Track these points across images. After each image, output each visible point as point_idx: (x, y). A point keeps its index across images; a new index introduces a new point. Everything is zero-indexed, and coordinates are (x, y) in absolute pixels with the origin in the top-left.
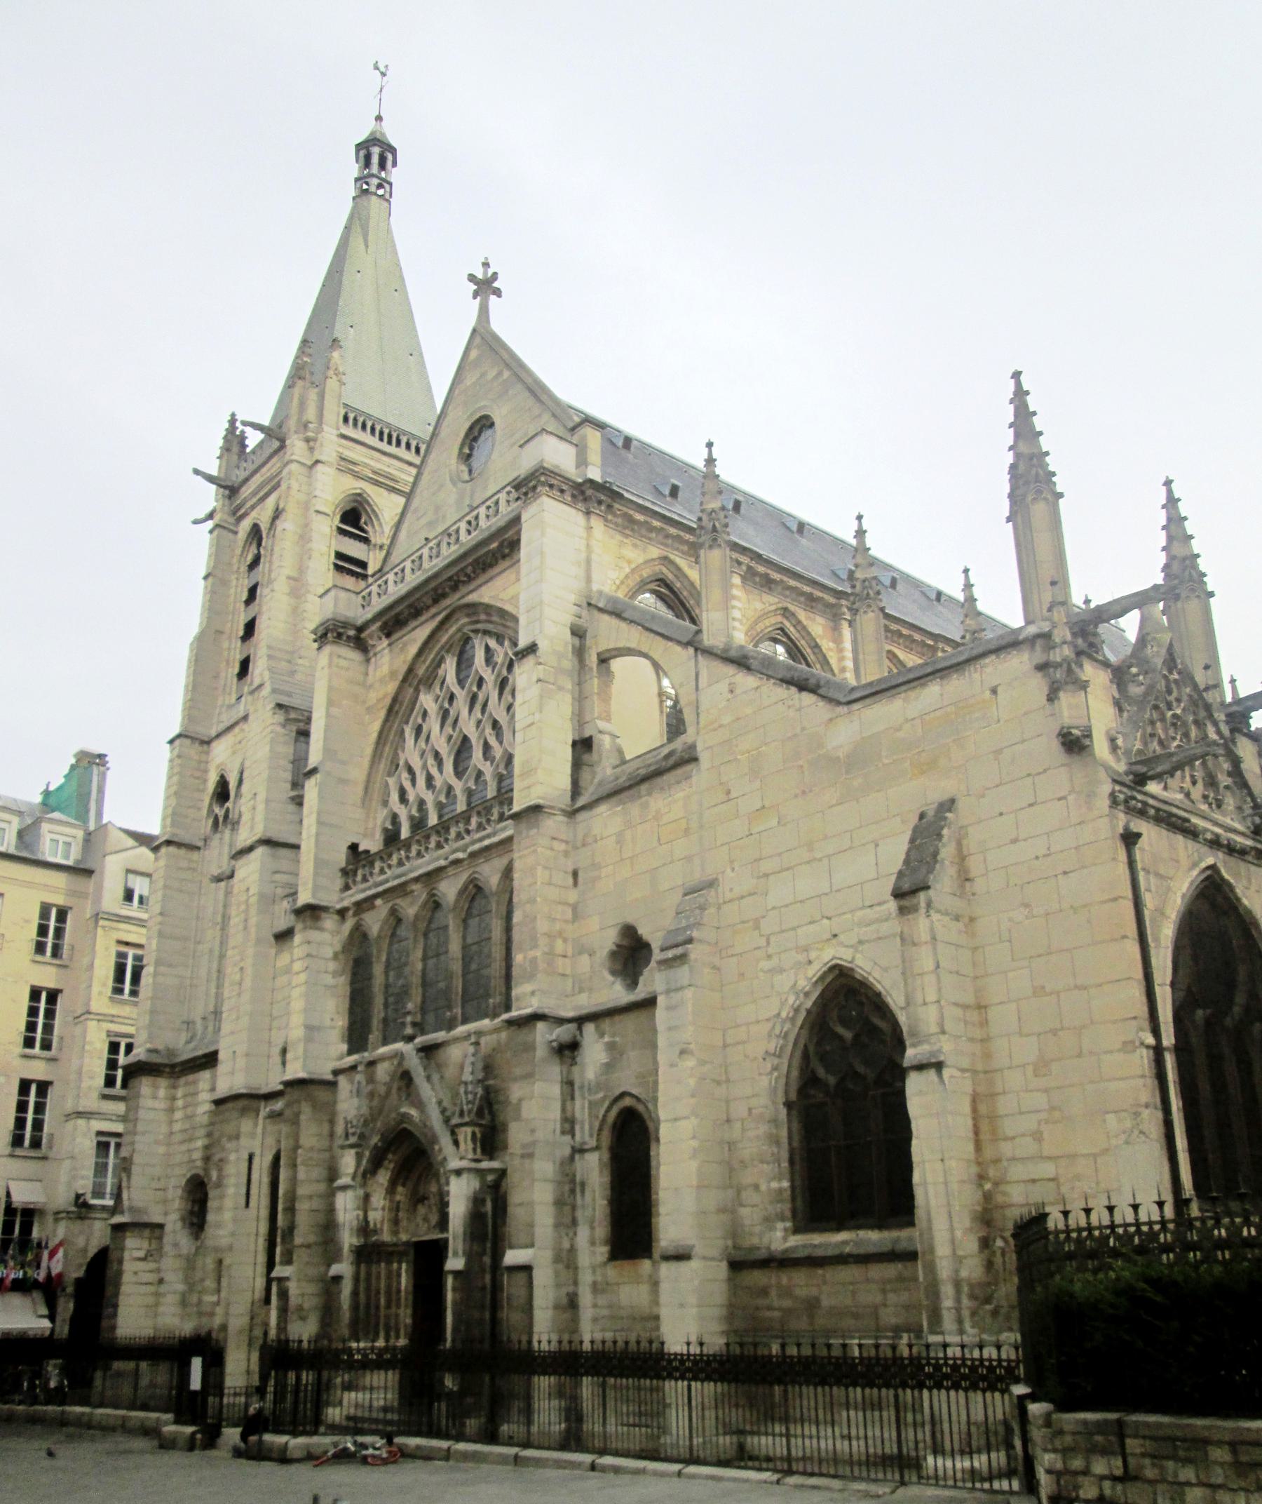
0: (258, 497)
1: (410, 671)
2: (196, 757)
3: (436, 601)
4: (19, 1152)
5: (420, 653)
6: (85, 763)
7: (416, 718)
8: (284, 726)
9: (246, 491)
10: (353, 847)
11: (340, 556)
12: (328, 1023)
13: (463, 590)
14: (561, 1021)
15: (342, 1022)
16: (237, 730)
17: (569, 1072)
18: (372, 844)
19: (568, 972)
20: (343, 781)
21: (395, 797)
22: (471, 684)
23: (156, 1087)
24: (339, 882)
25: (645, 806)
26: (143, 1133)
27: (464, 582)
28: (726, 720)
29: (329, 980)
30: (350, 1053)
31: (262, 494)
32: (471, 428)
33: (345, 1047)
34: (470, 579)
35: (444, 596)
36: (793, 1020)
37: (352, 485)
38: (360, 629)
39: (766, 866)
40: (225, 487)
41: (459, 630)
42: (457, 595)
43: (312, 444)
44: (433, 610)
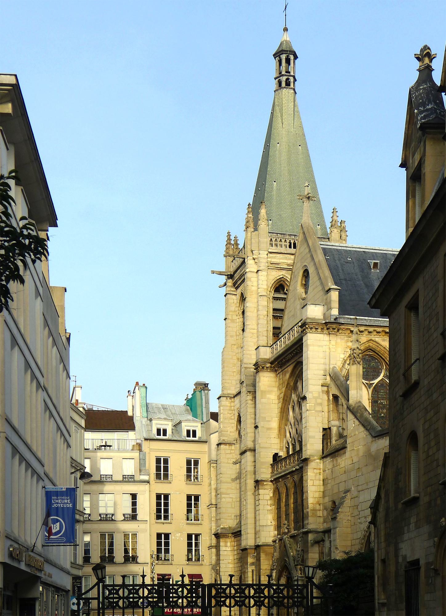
1: (288, 383)
2: (229, 405)
4: (190, 563)
6: (199, 389)
10: (276, 456)
11: (274, 310)
12: (270, 524)
14: (317, 532)
15: (274, 523)
17: (322, 549)
18: (282, 454)
19: (321, 515)
20: (269, 429)
21: (288, 435)
23: (226, 542)
24: (270, 470)
25: (337, 460)
26: (223, 560)
28: (353, 435)
29: (269, 508)
33: (276, 532)
36: (363, 539)
37: (276, 275)
38: (272, 363)
39: (360, 488)
43: (256, 260)
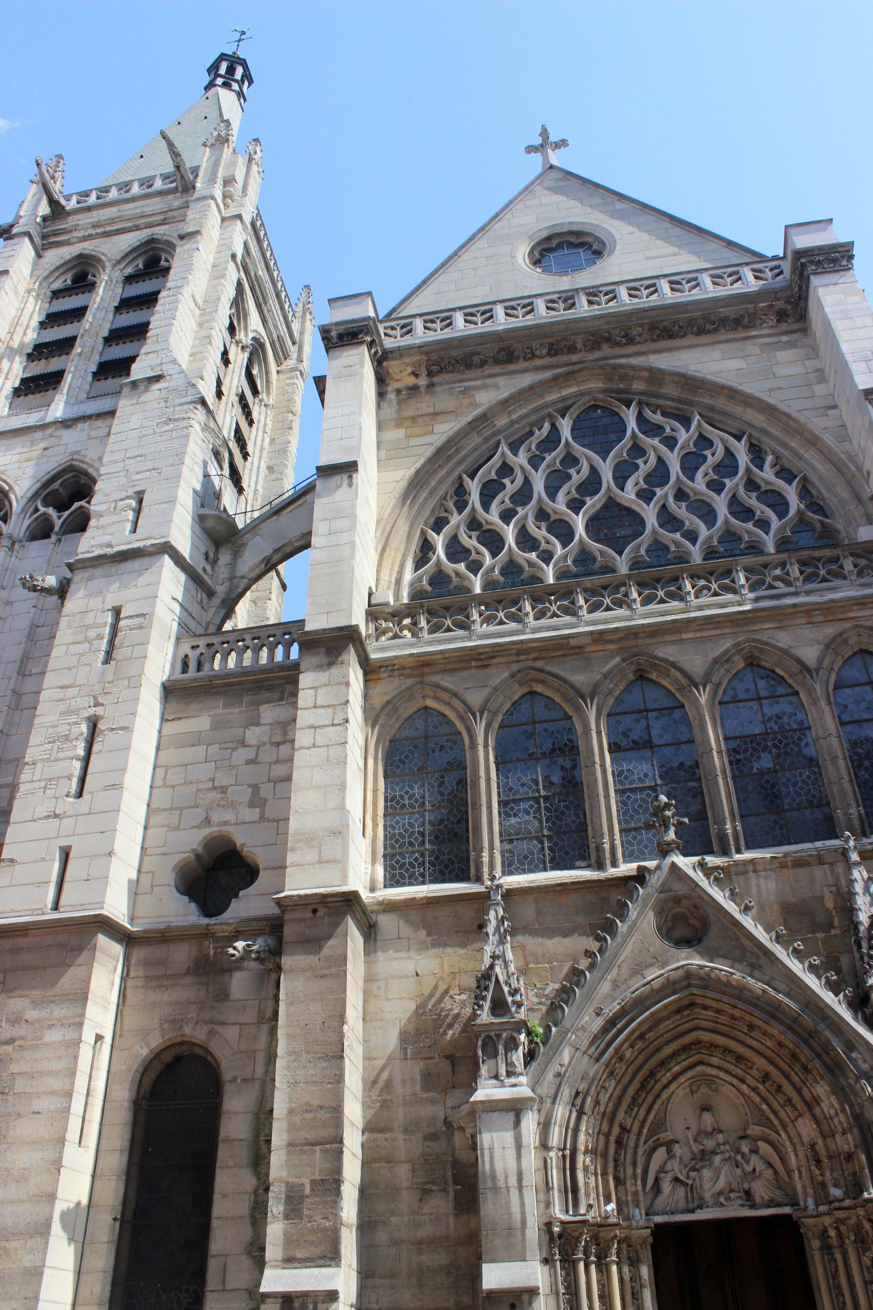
0: (99, 230)
3: (553, 351)
5: (505, 404)
7: (489, 471)
8: (203, 430)
9: (71, 221)
13: (606, 350)
16: (49, 431)
21: (440, 551)
22: (622, 449)
27: (618, 344)
30: (392, 881)
31: (108, 229)
32: (548, 239)
33: (380, 872)
34: (631, 341)
35: (572, 349)
40: (53, 203)
41: (582, 394)
42: (597, 354)
44: (538, 362)
